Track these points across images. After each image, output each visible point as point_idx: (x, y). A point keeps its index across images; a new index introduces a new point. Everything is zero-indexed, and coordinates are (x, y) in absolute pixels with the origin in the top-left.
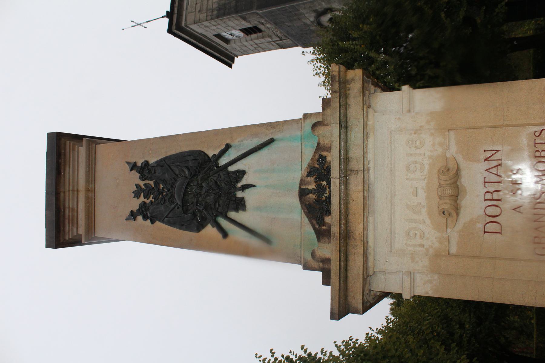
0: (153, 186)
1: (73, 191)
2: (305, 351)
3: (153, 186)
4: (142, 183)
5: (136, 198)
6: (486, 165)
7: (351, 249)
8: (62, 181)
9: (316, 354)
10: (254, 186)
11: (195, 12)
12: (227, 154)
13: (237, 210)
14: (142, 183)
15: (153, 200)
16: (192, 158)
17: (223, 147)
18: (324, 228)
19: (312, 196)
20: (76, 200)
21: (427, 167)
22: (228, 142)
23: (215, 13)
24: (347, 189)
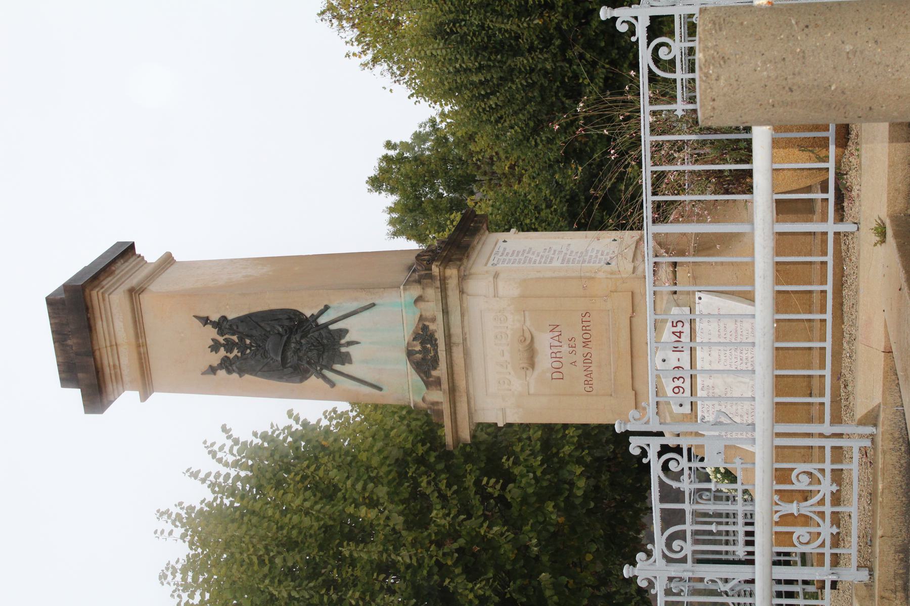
0: (237, 341)
1: (111, 346)
2: (297, 419)
3: (237, 341)
4: (221, 339)
5: (214, 353)
6: (552, 335)
7: (457, 398)
8: (95, 337)
9: (319, 421)
10: (357, 343)
12: (325, 314)
13: (343, 364)
14: (221, 339)
15: (239, 354)
16: (286, 316)
17: (322, 307)
18: (431, 379)
19: (419, 356)
20: (116, 356)
21: (509, 335)
22: (326, 303)
24: (451, 356)
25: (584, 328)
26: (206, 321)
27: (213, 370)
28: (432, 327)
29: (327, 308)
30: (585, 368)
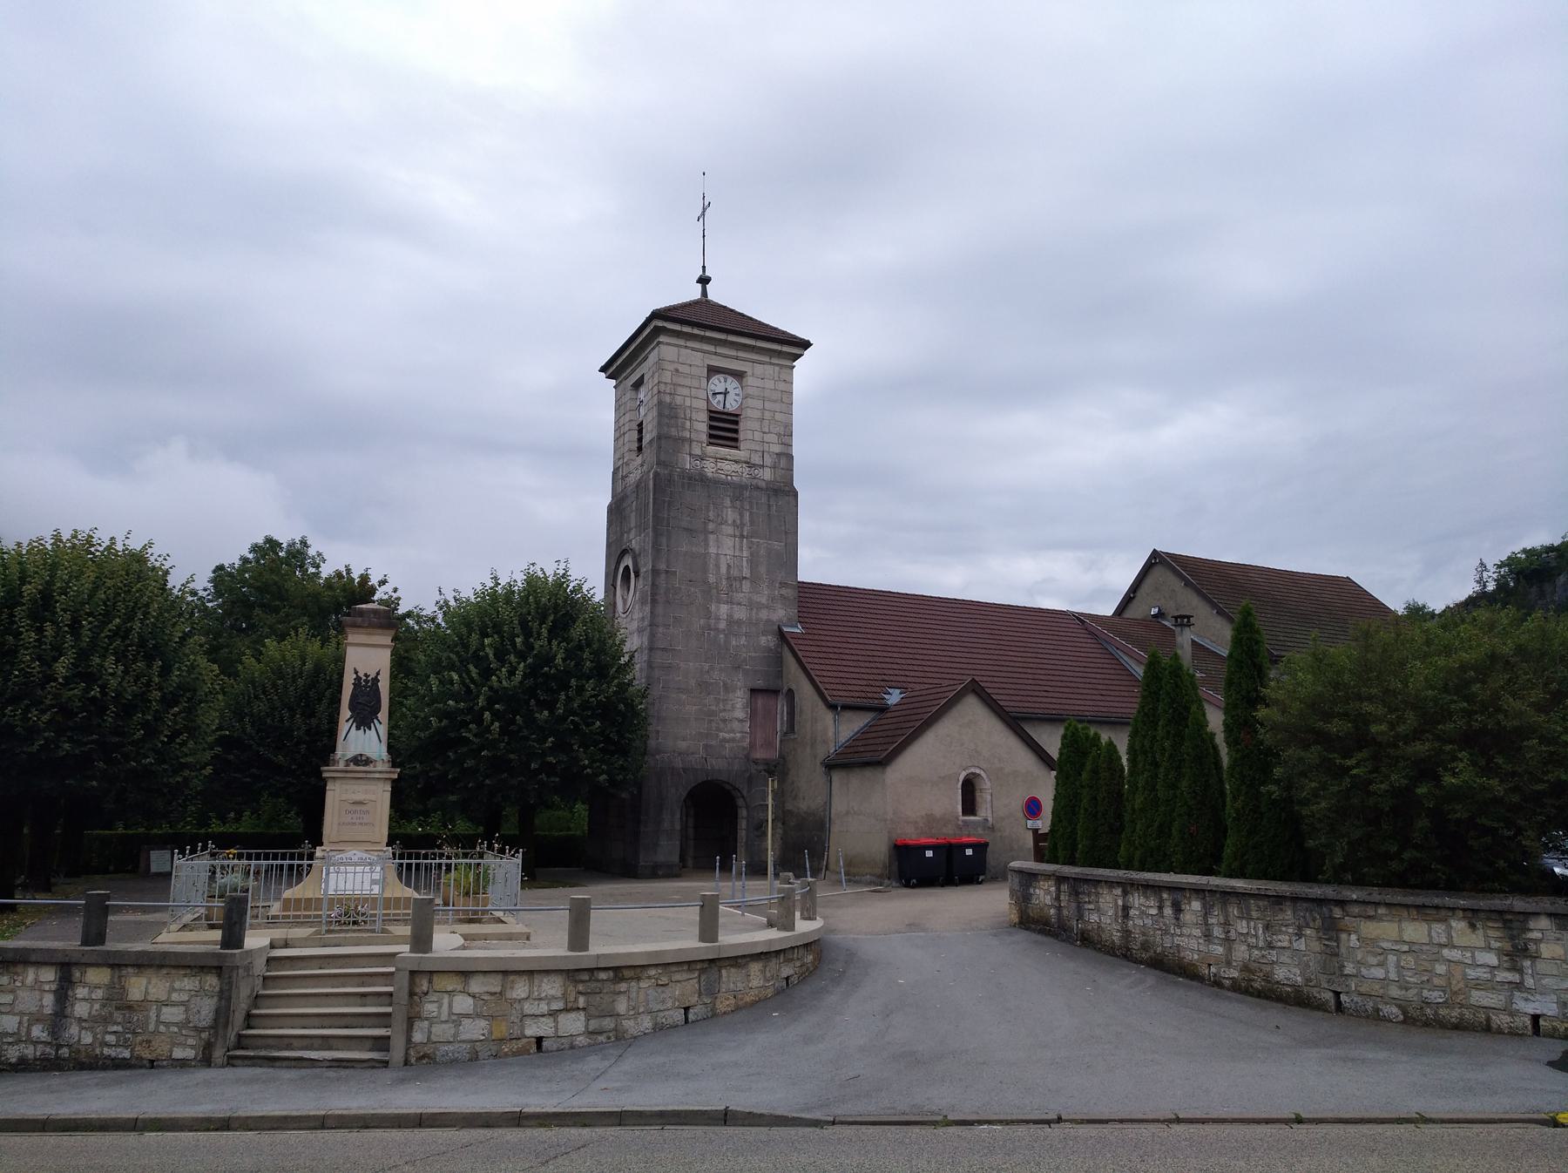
4: (369, 678)
11: (678, 362)
23: (668, 399)
26: (378, 674)
27: (356, 672)
28: (371, 765)
29: (381, 723)
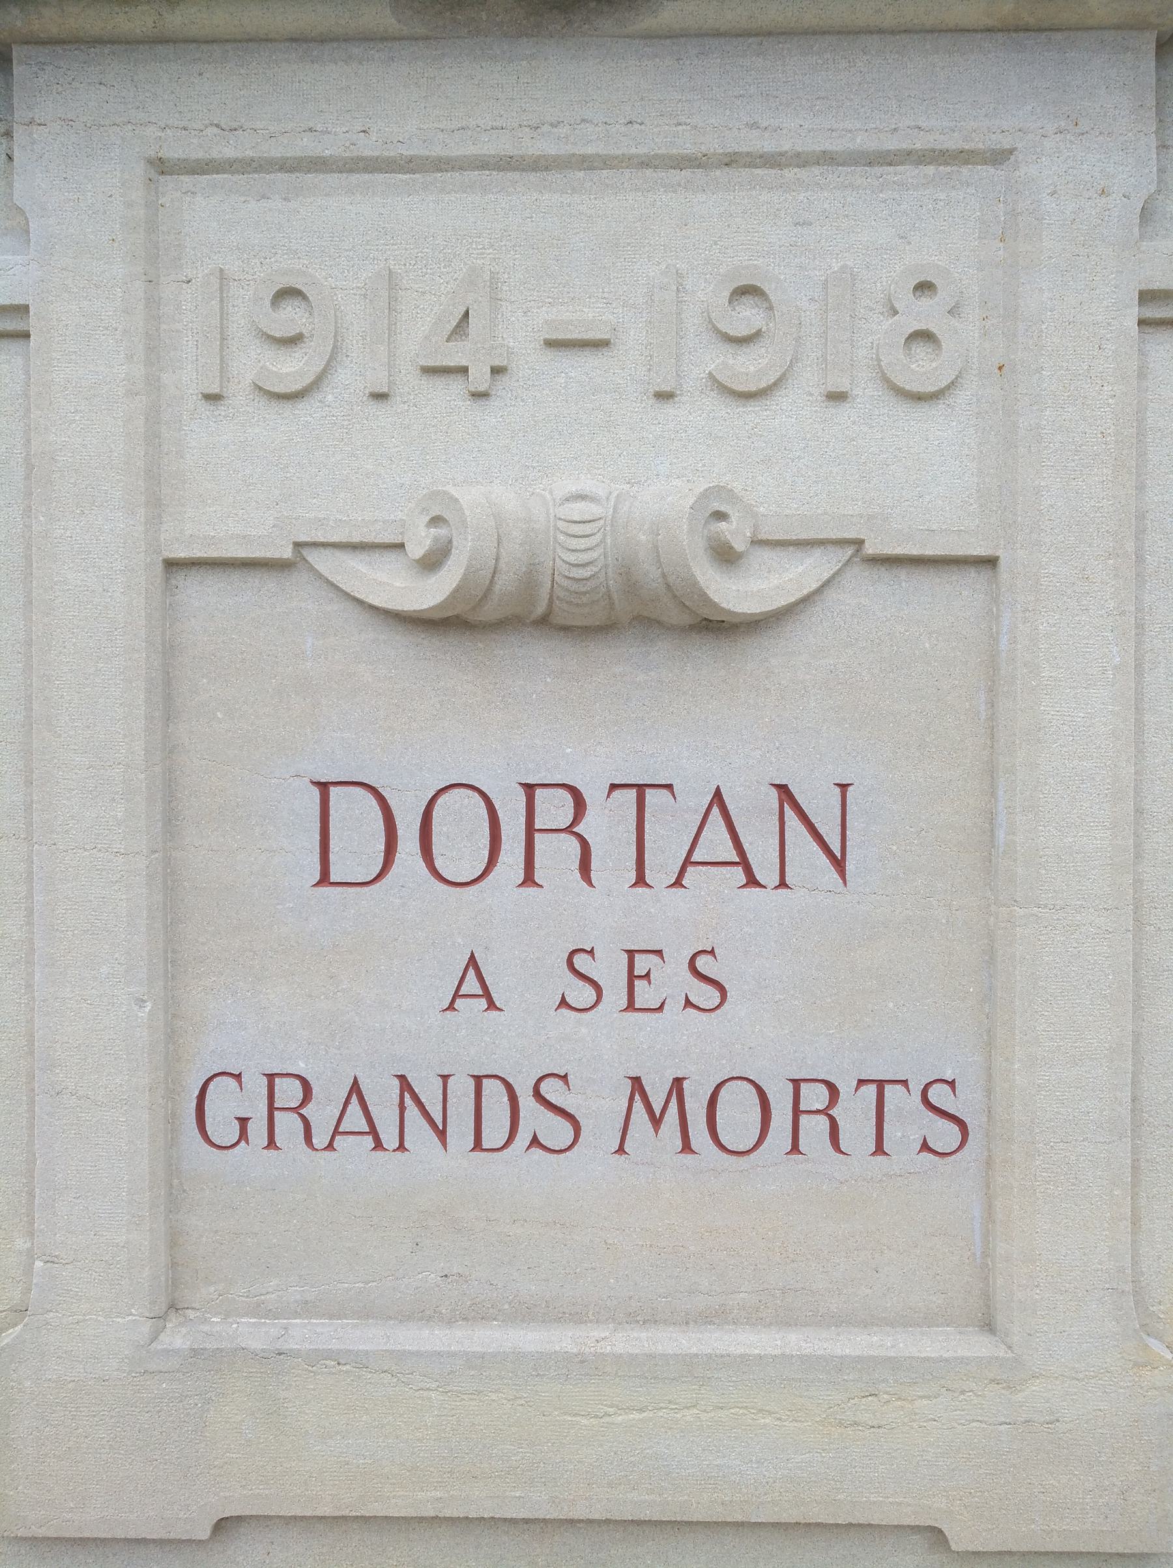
25: (813, 1097)
30: (431, 1096)
